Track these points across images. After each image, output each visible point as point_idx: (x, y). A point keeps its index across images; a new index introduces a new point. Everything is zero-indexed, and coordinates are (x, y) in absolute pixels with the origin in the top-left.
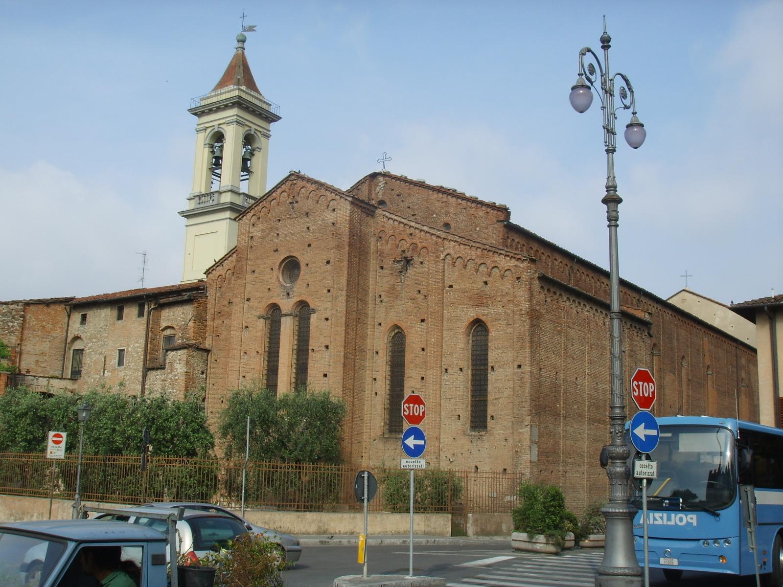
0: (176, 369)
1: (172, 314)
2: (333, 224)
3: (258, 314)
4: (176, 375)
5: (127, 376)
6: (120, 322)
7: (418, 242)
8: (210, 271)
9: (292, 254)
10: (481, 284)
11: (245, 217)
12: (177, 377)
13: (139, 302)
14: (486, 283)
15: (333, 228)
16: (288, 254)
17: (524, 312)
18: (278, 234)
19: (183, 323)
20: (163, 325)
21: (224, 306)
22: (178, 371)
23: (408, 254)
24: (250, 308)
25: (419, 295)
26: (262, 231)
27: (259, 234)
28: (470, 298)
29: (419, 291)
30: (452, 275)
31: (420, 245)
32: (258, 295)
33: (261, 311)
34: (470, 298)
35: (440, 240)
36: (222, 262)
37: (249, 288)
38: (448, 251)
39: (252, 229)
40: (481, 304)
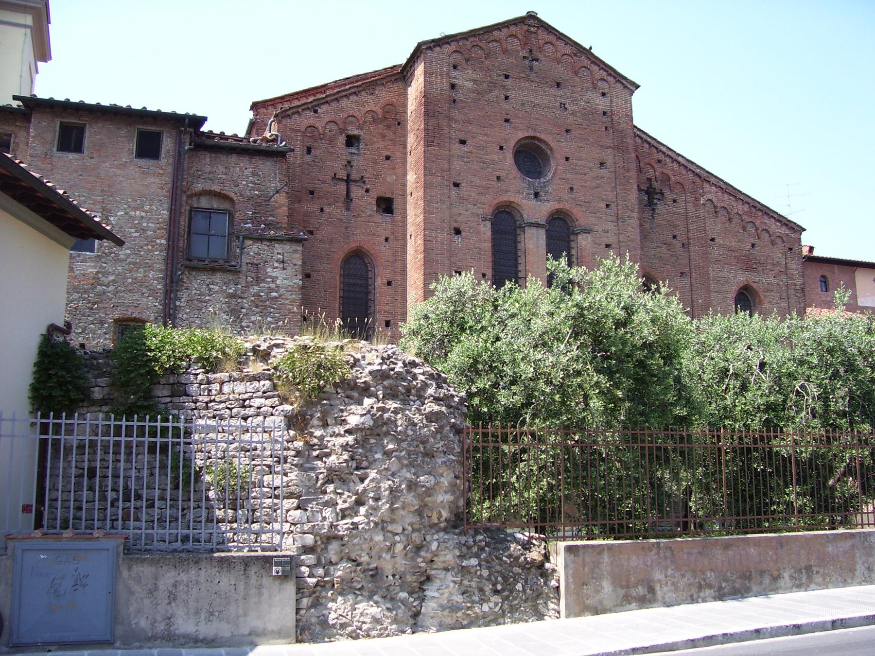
0: (270, 277)
1: (222, 169)
2: (605, 113)
3: (480, 211)
4: (271, 290)
5: (106, 274)
6: (72, 156)
7: (670, 173)
8: (290, 112)
9: (538, 135)
10: (749, 246)
11: (438, 49)
12: (274, 294)
13: (141, 127)
14: (753, 245)
15: (604, 119)
16: (531, 133)
17: (798, 288)
18: (507, 98)
19: (257, 192)
20: (199, 187)
21: (324, 182)
22: (278, 282)
23: (656, 185)
24: (462, 200)
25: (675, 241)
26: (475, 81)
27: (470, 85)
28: (738, 259)
29: (674, 237)
30: (715, 227)
31: (673, 179)
32: (477, 181)
33: (488, 210)
34: (738, 259)
35: (698, 180)
36: (316, 106)
37: (457, 165)
38: (709, 196)
39: (455, 73)
40: (750, 269)
